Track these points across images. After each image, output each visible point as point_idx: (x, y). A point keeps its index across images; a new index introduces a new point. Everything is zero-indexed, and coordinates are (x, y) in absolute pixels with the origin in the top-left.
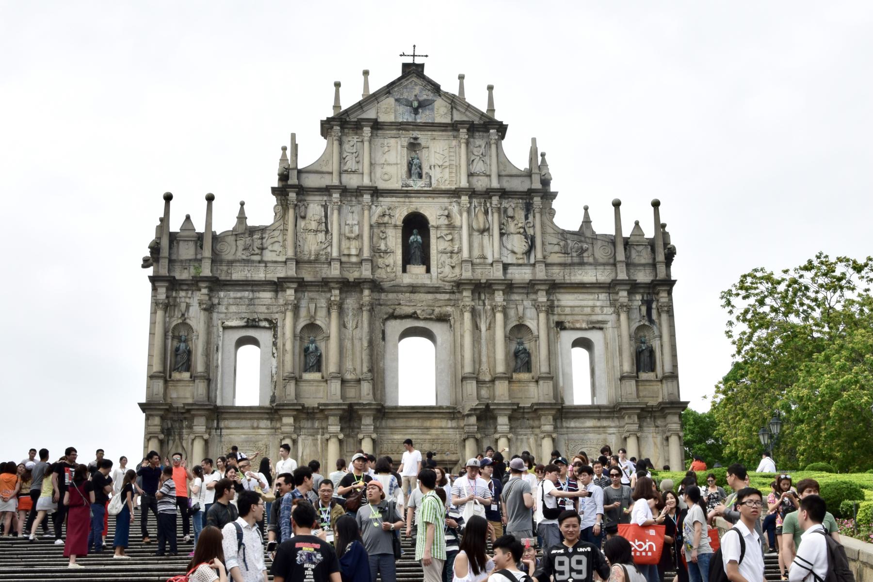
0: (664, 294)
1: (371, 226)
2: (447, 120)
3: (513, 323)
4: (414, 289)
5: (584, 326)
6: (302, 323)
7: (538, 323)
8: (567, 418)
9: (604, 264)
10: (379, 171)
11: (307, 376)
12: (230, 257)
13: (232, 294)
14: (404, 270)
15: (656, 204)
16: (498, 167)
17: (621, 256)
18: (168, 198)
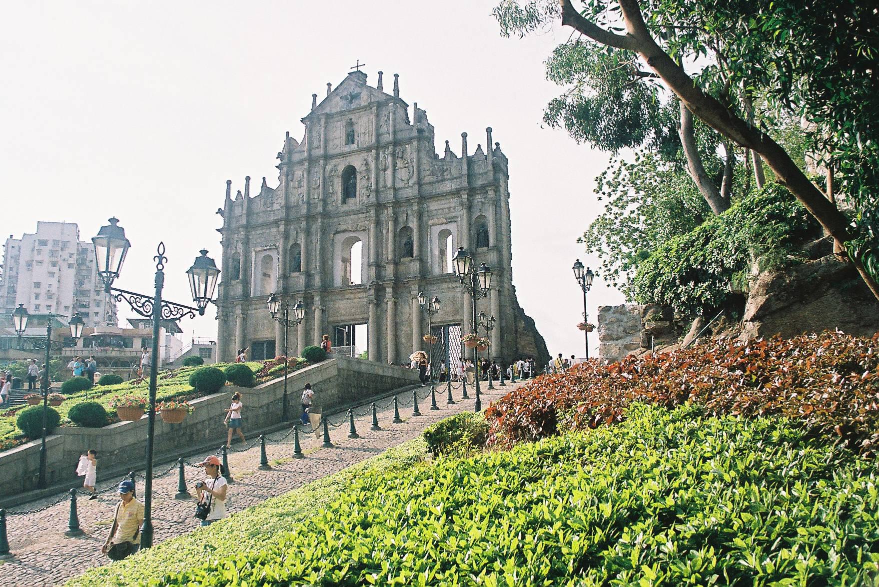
0: (491, 193)
1: (324, 179)
2: (366, 104)
3: (401, 226)
4: (347, 214)
5: (445, 221)
6: (291, 243)
7: (413, 224)
8: (431, 284)
9: (456, 178)
10: (331, 144)
11: (293, 275)
12: (258, 211)
13: (259, 232)
14: (344, 202)
15: (489, 131)
16: (394, 126)
17: (465, 172)
18: (229, 183)
